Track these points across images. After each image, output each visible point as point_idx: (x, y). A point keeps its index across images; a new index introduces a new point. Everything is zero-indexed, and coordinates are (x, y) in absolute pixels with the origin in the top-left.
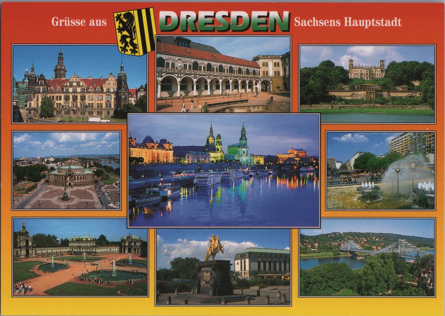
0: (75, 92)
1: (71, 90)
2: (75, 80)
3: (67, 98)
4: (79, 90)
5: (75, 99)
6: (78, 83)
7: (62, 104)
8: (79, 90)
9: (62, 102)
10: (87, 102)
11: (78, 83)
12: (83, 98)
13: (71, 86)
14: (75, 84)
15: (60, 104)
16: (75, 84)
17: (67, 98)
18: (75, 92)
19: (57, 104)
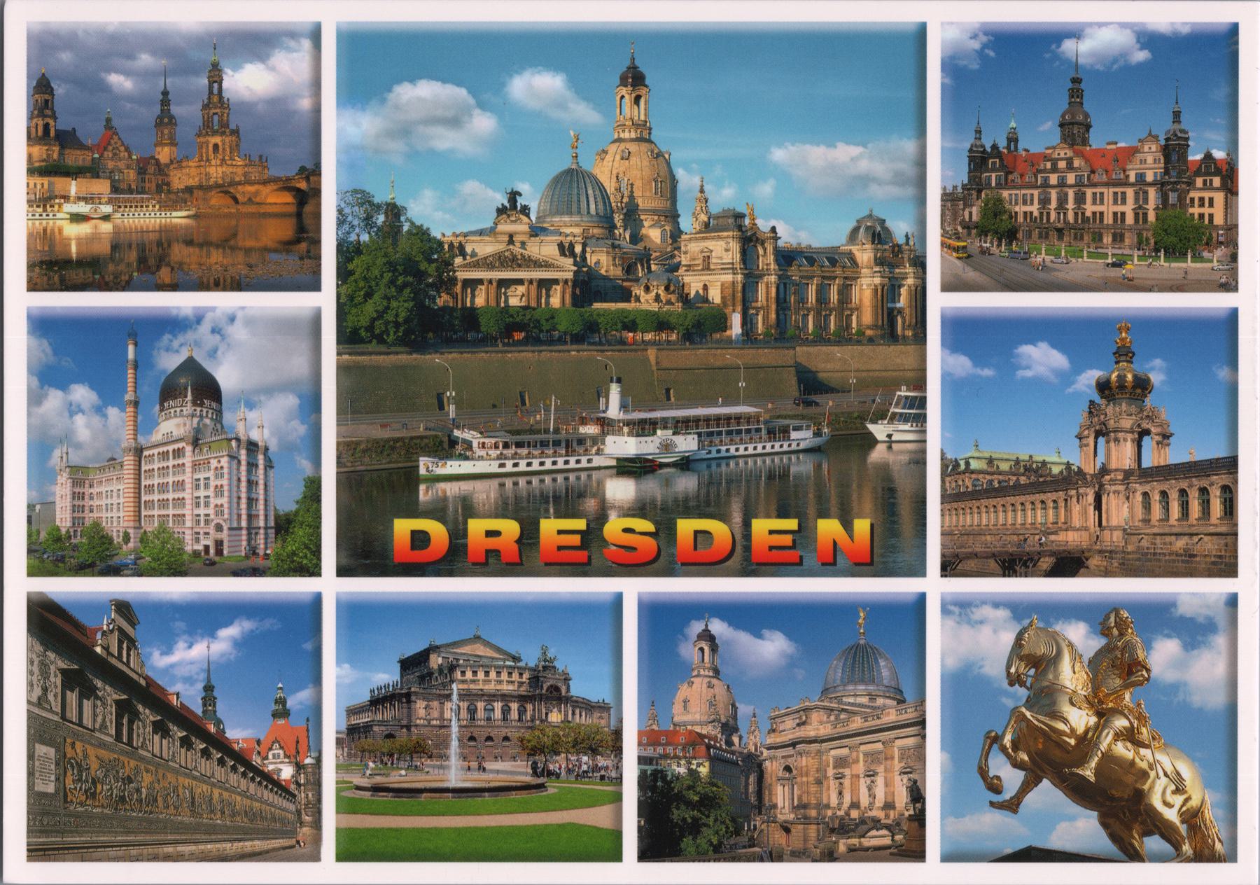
0: (1062, 184)
1: (1053, 179)
2: (1062, 155)
3: (1045, 201)
4: (1071, 178)
5: (1062, 201)
6: (1070, 161)
7: (1036, 214)
8: (1071, 178)
9: (1034, 208)
10: (1090, 208)
11: (1070, 161)
12: (1080, 199)
13: (1054, 169)
14: (1062, 165)
15: (1031, 213)
16: (1062, 165)
17: (1045, 201)
18: (1062, 184)
19: (1025, 213)
